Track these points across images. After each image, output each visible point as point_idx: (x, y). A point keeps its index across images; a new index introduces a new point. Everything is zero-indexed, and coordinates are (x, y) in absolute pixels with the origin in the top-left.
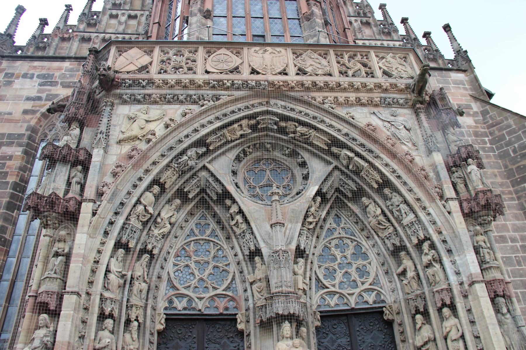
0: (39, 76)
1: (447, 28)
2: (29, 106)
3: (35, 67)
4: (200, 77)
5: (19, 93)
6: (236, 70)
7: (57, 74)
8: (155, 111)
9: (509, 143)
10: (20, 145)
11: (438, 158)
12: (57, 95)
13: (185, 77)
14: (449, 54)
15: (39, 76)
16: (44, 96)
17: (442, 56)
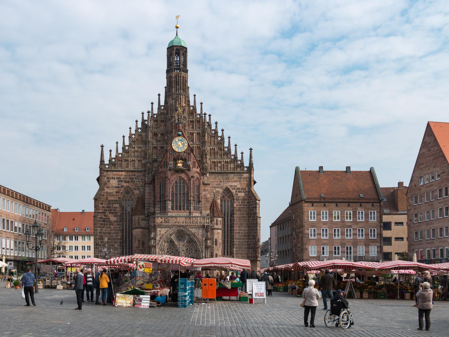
0: (117, 178)
1: (251, 149)
2: (116, 190)
3: (114, 175)
4: (170, 224)
5: (113, 185)
6: (176, 222)
7: (122, 177)
8: (163, 229)
9: (251, 205)
10: (118, 204)
11: (204, 239)
12: (124, 186)
13: (168, 224)
14: (246, 164)
15: (117, 178)
16: (120, 186)
17: (243, 166)
